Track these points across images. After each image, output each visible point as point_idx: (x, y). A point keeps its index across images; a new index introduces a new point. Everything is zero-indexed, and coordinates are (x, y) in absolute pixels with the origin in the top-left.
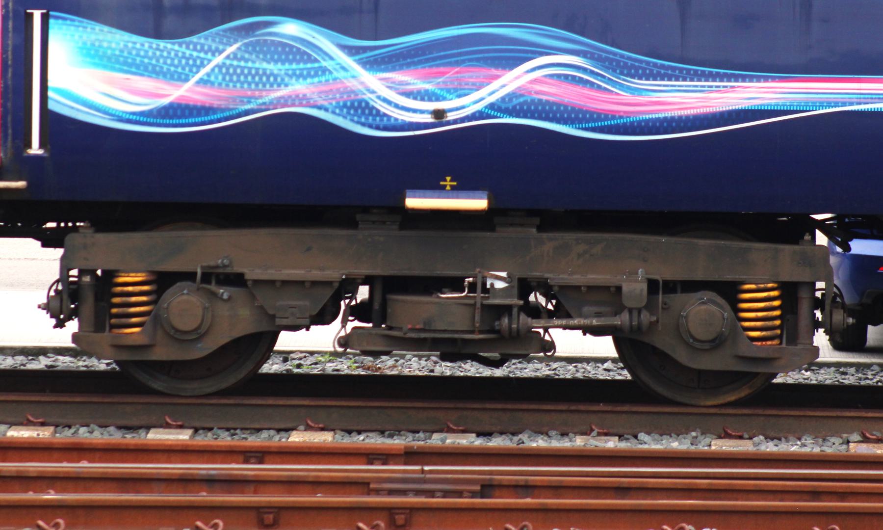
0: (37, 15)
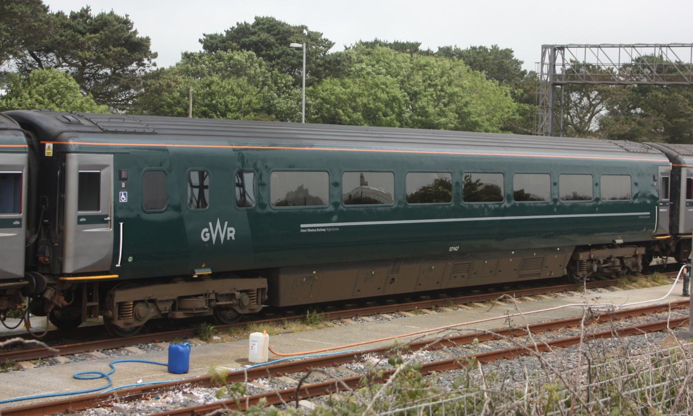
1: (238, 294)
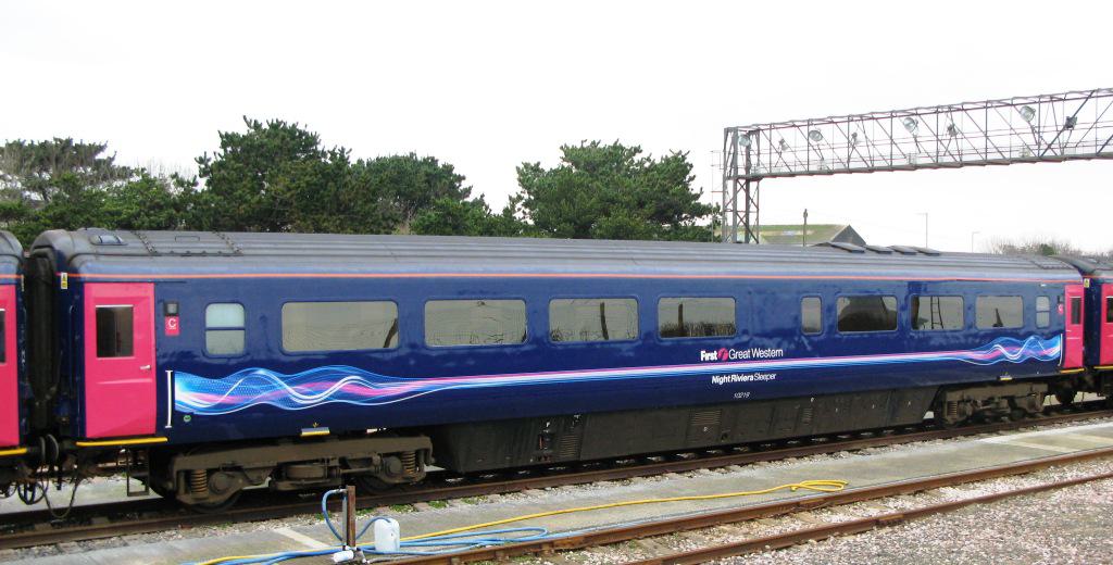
0: (169, 372)
1: (376, 458)
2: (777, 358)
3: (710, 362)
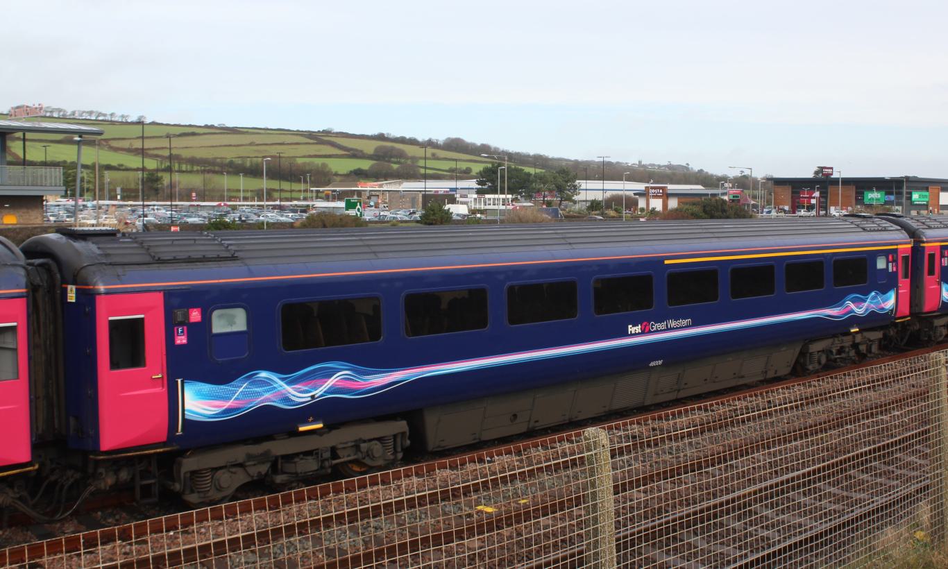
0: (179, 381)
2: (687, 327)
3: (636, 335)
